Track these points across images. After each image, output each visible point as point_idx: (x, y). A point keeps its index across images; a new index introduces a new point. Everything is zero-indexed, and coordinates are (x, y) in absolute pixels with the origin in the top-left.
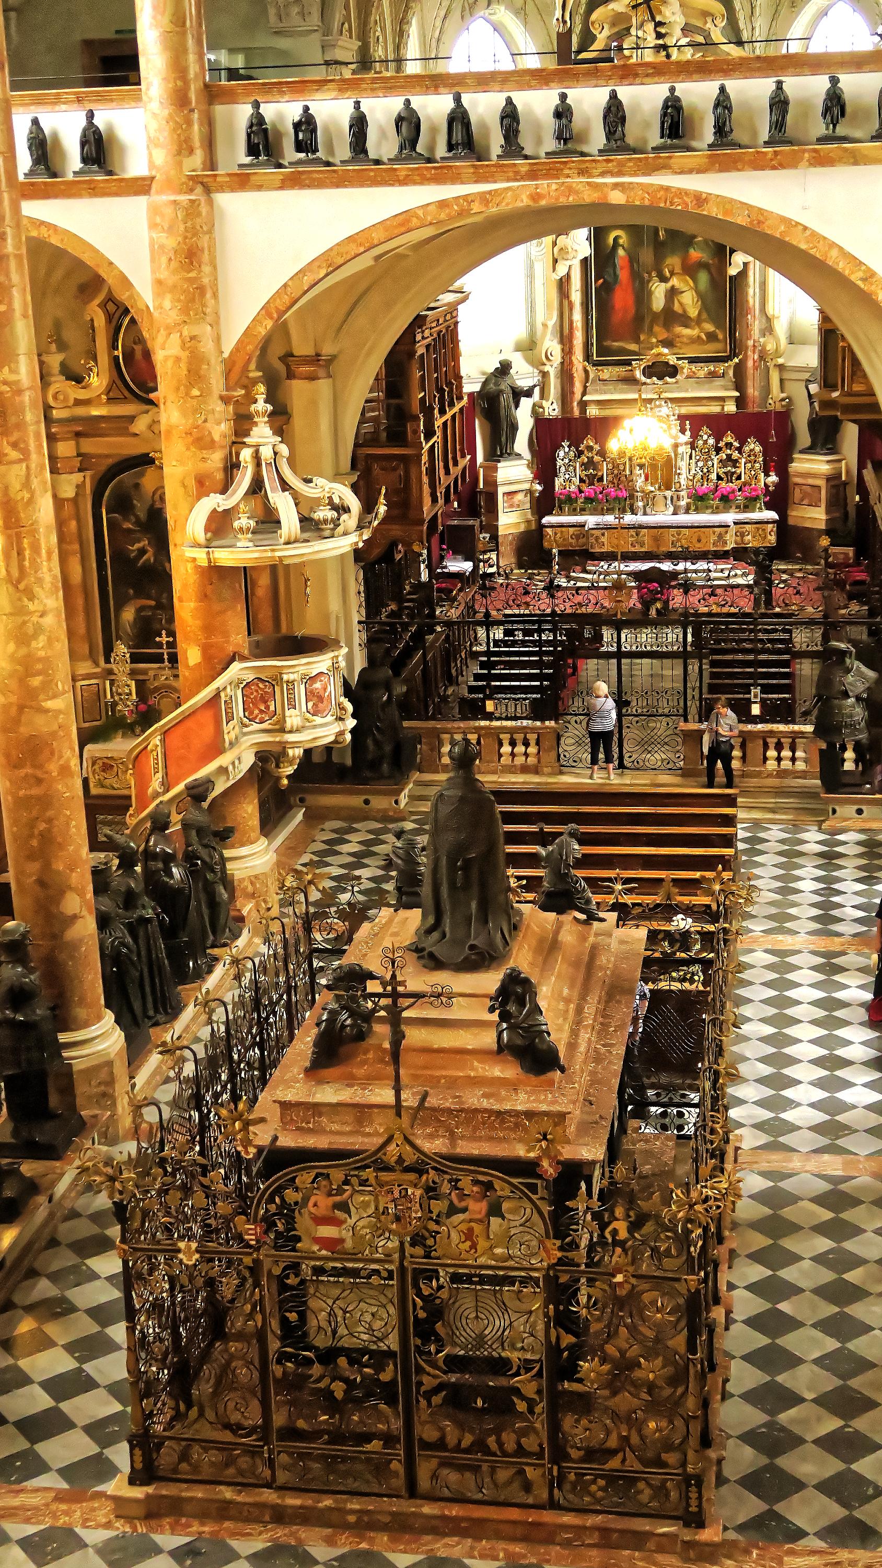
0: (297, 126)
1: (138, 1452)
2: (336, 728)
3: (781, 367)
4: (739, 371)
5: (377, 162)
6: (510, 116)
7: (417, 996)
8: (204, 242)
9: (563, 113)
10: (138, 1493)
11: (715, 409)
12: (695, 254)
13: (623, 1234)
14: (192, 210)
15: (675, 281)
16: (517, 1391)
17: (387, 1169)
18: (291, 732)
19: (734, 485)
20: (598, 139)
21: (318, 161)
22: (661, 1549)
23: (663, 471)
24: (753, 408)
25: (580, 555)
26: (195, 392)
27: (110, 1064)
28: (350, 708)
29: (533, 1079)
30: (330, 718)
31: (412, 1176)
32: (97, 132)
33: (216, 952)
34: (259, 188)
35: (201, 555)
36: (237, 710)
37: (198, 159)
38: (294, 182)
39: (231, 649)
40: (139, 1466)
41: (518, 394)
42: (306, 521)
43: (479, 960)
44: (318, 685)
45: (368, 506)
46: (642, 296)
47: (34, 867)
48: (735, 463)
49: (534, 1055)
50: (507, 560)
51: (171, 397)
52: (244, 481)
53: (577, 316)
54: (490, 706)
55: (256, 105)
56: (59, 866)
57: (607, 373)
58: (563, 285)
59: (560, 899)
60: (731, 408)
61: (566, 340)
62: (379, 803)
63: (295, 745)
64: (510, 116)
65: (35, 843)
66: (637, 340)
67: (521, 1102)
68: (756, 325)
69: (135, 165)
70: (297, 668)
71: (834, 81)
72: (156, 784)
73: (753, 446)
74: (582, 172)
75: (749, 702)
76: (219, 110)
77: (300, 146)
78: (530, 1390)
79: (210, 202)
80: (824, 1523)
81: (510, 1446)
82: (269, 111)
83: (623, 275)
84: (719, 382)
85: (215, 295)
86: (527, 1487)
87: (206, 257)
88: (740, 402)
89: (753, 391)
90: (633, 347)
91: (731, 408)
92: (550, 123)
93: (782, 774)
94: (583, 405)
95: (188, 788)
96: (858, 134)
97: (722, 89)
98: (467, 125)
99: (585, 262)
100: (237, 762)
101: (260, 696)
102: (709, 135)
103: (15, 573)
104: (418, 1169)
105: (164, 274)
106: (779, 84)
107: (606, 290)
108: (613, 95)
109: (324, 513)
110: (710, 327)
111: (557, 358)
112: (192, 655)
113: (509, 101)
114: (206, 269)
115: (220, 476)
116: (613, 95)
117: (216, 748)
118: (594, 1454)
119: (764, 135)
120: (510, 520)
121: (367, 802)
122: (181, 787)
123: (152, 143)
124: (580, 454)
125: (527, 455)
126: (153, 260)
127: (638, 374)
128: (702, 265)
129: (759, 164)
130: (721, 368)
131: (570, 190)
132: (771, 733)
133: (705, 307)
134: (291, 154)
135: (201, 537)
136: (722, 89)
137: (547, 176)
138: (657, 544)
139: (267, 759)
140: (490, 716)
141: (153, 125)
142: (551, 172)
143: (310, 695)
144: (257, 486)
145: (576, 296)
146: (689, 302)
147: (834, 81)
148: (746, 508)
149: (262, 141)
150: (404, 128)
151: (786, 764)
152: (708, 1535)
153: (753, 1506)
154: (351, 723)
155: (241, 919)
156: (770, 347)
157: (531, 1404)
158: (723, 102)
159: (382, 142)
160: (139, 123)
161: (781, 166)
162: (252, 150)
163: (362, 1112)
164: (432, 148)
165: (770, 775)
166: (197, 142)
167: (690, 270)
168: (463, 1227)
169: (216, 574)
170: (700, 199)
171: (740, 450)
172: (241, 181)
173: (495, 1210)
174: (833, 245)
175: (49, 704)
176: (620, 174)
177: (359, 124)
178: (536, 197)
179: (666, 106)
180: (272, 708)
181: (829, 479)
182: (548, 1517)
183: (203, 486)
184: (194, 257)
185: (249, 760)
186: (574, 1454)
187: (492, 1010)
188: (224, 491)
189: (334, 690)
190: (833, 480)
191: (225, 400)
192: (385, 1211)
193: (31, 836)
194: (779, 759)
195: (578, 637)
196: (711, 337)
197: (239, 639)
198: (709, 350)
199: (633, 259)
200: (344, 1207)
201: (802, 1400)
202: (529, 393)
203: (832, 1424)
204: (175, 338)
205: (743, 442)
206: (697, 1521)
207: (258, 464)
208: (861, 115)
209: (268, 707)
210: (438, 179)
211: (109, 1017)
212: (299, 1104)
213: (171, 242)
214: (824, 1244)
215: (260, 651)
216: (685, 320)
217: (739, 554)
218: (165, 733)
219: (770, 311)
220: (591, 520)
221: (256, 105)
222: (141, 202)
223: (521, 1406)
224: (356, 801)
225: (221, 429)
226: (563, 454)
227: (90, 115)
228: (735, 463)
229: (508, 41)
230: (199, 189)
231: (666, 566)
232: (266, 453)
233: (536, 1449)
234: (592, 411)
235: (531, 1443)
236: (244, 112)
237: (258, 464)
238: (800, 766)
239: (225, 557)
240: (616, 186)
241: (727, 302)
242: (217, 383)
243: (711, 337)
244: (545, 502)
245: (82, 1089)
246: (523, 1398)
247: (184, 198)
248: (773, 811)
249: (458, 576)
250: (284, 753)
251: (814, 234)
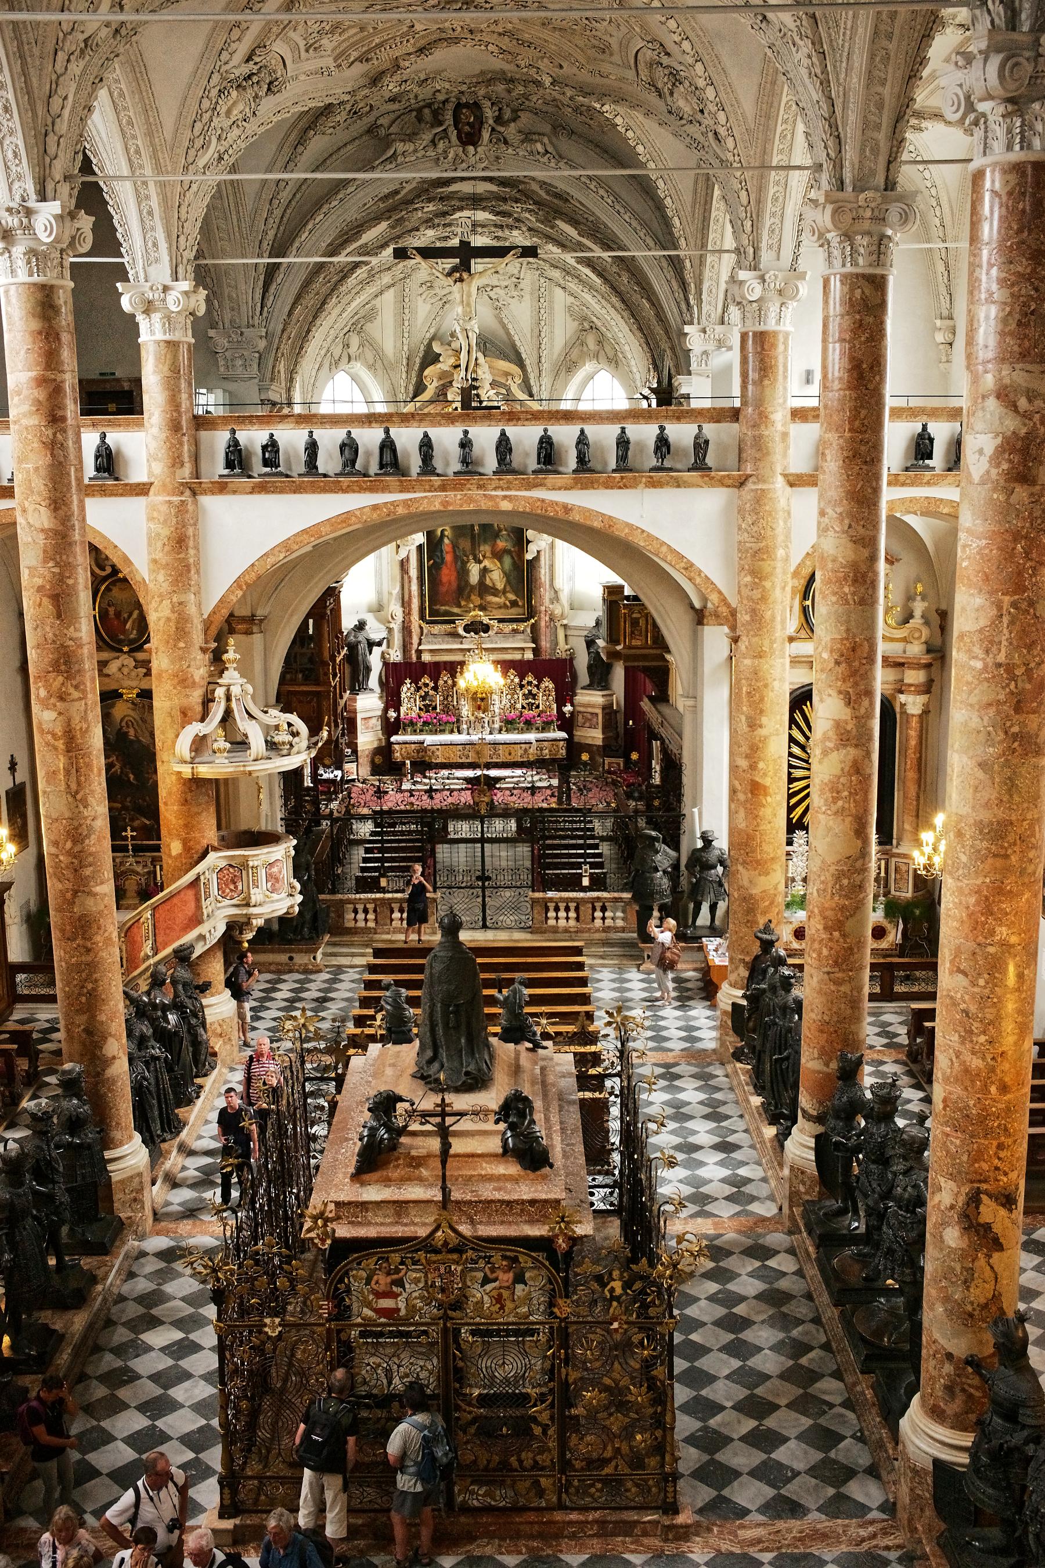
0: (264, 448)
1: (226, 1491)
2: (289, 902)
3: (565, 626)
4: (534, 628)
5: (325, 476)
6: (426, 446)
7: (461, 1114)
8: (190, 531)
9: (465, 444)
10: (228, 1524)
11: (518, 656)
12: (501, 544)
13: (619, 1291)
14: (182, 507)
15: (486, 563)
16: (534, 1419)
17: (436, 1251)
19: (534, 713)
20: (491, 463)
21: (281, 474)
22: (645, 1534)
23: (481, 701)
24: (546, 656)
25: (423, 765)
26: (182, 645)
27: (140, 1175)
28: (298, 886)
29: (532, 1175)
30: (284, 895)
31: (455, 1256)
32: (108, 448)
33: (198, 1081)
34: (234, 492)
35: (186, 771)
37: (187, 470)
38: (262, 488)
39: (205, 842)
40: (227, 1502)
41: (371, 644)
42: (272, 746)
43: (477, 1082)
44: (275, 870)
45: (314, 731)
46: (463, 573)
47: (81, 1019)
48: (534, 696)
49: (531, 1156)
50: (365, 771)
51: (162, 648)
52: (218, 711)
53: (415, 587)
54: (383, 882)
55: (233, 432)
56: (102, 1017)
57: (437, 629)
58: (403, 565)
59: (517, 1032)
60: (529, 656)
61: (405, 604)
62: (301, 959)
63: (258, 916)
64: (426, 446)
65: (83, 999)
66: (459, 606)
67: (526, 1191)
68: (546, 594)
69: (138, 472)
70: (260, 856)
71: (662, 428)
72: (147, 948)
73: (548, 683)
74: (480, 487)
75: (581, 876)
76: (204, 434)
77: (266, 463)
78: (544, 1417)
79: (196, 503)
80: (760, 1502)
81: (528, 1463)
82: (242, 436)
83: (448, 558)
84: (520, 636)
85: (198, 572)
86: (541, 1493)
87: (191, 543)
88: (536, 651)
89: (545, 644)
90: (456, 610)
91: (529, 656)
92: (456, 451)
93: (606, 930)
94: (419, 652)
95: (175, 951)
96: (679, 466)
97: (582, 431)
98: (394, 451)
99: (420, 548)
101: (234, 877)
102: (572, 463)
103: (74, 786)
104: (459, 1250)
105: (159, 555)
106: (623, 429)
107: (435, 569)
108: (503, 433)
109: (283, 737)
110: (512, 596)
111: (399, 617)
112: (174, 847)
113: (426, 435)
114: (192, 552)
115: (199, 708)
116: (503, 433)
117: (197, 920)
118: (595, 1463)
119: (613, 464)
120: (367, 739)
121: (291, 958)
122: (169, 950)
123: (151, 458)
124: (418, 689)
125: (378, 689)
126: (150, 545)
127: (461, 631)
128: (506, 551)
129: (608, 485)
130: (522, 627)
131: (471, 500)
132: (598, 899)
133: (508, 582)
134: (258, 467)
135: (187, 755)
136: (582, 431)
137: (455, 489)
138: (474, 758)
139: (234, 927)
140: (384, 891)
141: (153, 445)
142: (458, 487)
143: (269, 877)
144: (228, 714)
145: (413, 572)
146: (497, 578)
147: (662, 428)
148: (543, 730)
149: (236, 458)
150: (347, 451)
151: (609, 922)
152: (681, 1519)
153: (706, 1494)
154: (299, 898)
155: (215, 1054)
156: (558, 611)
157: (545, 1428)
158: (582, 440)
159: (328, 461)
160: (141, 445)
161: (626, 487)
162: (229, 465)
163: (400, 1207)
164: (366, 466)
165: (597, 931)
166: (186, 459)
167: (498, 555)
168: (495, 1293)
169: (196, 783)
170: (567, 509)
171: (538, 687)
172: (221, 488)
173: (520, 1279)
174: (663, 543)
175: (98, 889)
176: (508, 489)
177: (312, 448)
178: (445, 504)
179: (541, 442)
181: (604, 708)
182: (558, 1516)
183: (185, 717)
184: (182, 544)
185: (222, 928)
186: (578, 1464)
187: (497, 1122)
188: (202, 720)
189: (286, 871)
190: (607, 709)
191: (204, 650)
192: (433, 1285)
193: (80, 994)
194: (604, 918)
195: (433, 825)
196: (514, 604)
197: (210, 834)
198: (513, 612)
199: (455, 546)
200: (400, 1283)
201: (722, 1408)
202: (379, 644)
203: (750, 1424)
204: (166, 603)
205: (540, 681)
206: (672, 1508)
207: (228, 698)
208: (682, 452)
210: (372, 489)
211: (137, 1137)
212: (350, 1203)
213: (165, 532)
214: (713, 1287)
215: (227, 843)
216: (495, 592)
217: (539, 764)
218: (154, 909)
219: (559, 584)
220: (429, 739)
221: (233, 432)
222: (141, 502)
223: (537, 1431)
224: (283, 958)
225: (200, 670)
226: (407, 689)
227: (103, 436)
228: (534, 696)
229: (363, 388)
230: (188, 492)
231: (493, 773)
232: (235, 690)
233: (548, 1463)
234: (426, 658)
235: (544, 1459)
236: (222, 438)
237: (228, 698)
238: (620, 923)
239: (205, 771)
240: (505, 497)
241: (525, 577)
242: (197, 637)
243: (514, 604)
244: (391, 727)
245: (118, 1196)
246: (538, 1424)
247: (176, 499)
248: (602, 957)
249: (333, 781)
250: (248, 923)
251: (649, 535)
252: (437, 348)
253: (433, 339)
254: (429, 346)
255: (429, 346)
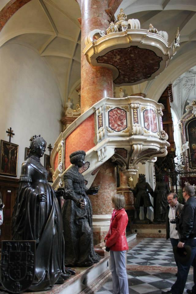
18: (135, 134)
36: (105, 122)
99: (188, 150)
100: (103, 150)
121: (160, 231)
180: (125, 124)
185: (110, 152)
209: (122, 123)
252: (188, 102)
253: (187, 100)
254: (186, 101)
255: (186, 101)
